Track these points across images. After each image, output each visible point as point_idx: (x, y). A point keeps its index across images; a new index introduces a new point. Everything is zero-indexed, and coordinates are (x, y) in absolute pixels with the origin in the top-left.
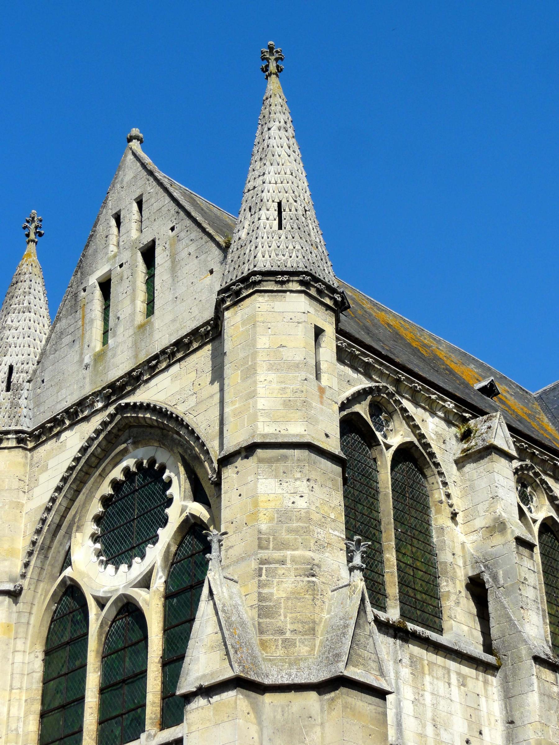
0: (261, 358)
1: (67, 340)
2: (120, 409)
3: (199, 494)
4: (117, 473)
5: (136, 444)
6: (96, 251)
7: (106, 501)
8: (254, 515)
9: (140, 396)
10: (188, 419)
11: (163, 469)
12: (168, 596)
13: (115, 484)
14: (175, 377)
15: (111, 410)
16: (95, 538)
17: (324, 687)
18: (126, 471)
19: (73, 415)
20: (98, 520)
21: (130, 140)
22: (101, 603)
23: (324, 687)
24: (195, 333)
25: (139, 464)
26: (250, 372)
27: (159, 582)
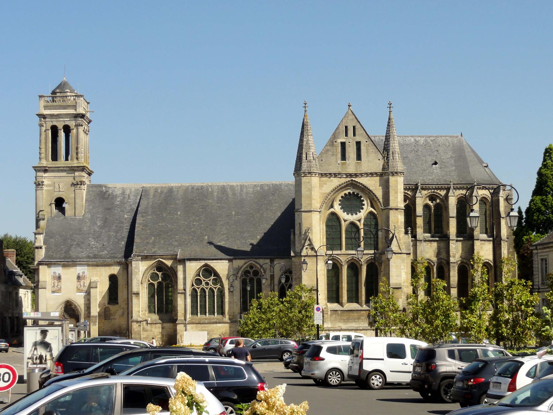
0: (399, 191)
1: (330, 153)
2: (352, 180)
3: (372, 206)
4: (347, 192)
5: (354, 188)
6: (339, 133)
7: (342, 197)
8: (398, 222)
9: (357, 179)
10: (374, 192)
11: (361, 197)
12: (364, 225)
13: (345, 194)
14: (369, 180)
15: (350, 179)
16: (340, 205)
17: (407, 254)
18: (349, 193)
19: (336, 175)
20: (340, 201)
21: (349, 106)
22: (345, 221)
23: (407, 254)
24: (376, 173)
25: (353, 193)
26: (396, 193)
27: (362, 221)
